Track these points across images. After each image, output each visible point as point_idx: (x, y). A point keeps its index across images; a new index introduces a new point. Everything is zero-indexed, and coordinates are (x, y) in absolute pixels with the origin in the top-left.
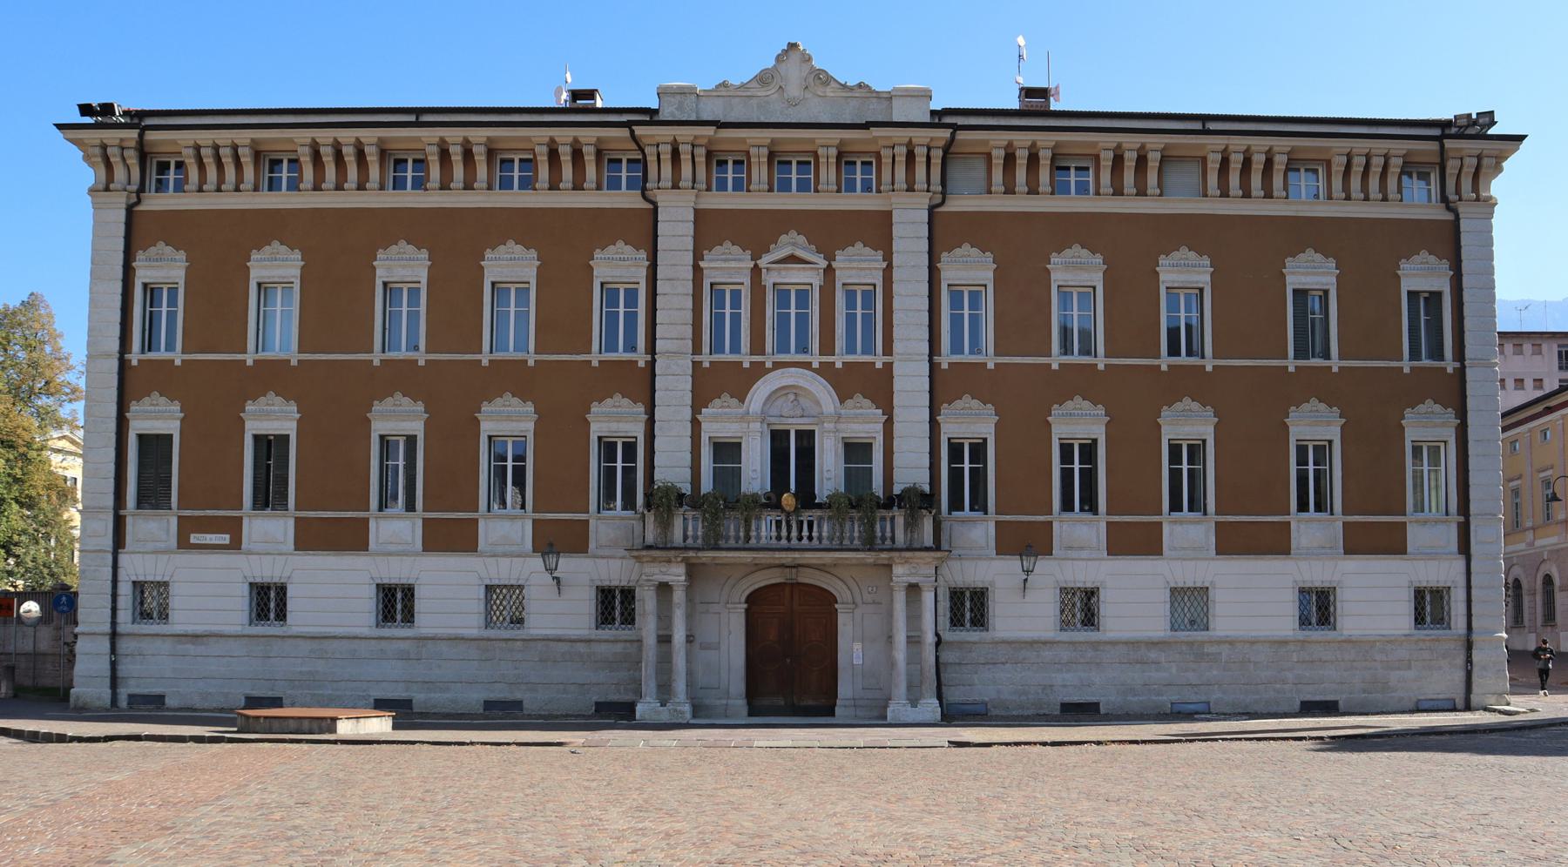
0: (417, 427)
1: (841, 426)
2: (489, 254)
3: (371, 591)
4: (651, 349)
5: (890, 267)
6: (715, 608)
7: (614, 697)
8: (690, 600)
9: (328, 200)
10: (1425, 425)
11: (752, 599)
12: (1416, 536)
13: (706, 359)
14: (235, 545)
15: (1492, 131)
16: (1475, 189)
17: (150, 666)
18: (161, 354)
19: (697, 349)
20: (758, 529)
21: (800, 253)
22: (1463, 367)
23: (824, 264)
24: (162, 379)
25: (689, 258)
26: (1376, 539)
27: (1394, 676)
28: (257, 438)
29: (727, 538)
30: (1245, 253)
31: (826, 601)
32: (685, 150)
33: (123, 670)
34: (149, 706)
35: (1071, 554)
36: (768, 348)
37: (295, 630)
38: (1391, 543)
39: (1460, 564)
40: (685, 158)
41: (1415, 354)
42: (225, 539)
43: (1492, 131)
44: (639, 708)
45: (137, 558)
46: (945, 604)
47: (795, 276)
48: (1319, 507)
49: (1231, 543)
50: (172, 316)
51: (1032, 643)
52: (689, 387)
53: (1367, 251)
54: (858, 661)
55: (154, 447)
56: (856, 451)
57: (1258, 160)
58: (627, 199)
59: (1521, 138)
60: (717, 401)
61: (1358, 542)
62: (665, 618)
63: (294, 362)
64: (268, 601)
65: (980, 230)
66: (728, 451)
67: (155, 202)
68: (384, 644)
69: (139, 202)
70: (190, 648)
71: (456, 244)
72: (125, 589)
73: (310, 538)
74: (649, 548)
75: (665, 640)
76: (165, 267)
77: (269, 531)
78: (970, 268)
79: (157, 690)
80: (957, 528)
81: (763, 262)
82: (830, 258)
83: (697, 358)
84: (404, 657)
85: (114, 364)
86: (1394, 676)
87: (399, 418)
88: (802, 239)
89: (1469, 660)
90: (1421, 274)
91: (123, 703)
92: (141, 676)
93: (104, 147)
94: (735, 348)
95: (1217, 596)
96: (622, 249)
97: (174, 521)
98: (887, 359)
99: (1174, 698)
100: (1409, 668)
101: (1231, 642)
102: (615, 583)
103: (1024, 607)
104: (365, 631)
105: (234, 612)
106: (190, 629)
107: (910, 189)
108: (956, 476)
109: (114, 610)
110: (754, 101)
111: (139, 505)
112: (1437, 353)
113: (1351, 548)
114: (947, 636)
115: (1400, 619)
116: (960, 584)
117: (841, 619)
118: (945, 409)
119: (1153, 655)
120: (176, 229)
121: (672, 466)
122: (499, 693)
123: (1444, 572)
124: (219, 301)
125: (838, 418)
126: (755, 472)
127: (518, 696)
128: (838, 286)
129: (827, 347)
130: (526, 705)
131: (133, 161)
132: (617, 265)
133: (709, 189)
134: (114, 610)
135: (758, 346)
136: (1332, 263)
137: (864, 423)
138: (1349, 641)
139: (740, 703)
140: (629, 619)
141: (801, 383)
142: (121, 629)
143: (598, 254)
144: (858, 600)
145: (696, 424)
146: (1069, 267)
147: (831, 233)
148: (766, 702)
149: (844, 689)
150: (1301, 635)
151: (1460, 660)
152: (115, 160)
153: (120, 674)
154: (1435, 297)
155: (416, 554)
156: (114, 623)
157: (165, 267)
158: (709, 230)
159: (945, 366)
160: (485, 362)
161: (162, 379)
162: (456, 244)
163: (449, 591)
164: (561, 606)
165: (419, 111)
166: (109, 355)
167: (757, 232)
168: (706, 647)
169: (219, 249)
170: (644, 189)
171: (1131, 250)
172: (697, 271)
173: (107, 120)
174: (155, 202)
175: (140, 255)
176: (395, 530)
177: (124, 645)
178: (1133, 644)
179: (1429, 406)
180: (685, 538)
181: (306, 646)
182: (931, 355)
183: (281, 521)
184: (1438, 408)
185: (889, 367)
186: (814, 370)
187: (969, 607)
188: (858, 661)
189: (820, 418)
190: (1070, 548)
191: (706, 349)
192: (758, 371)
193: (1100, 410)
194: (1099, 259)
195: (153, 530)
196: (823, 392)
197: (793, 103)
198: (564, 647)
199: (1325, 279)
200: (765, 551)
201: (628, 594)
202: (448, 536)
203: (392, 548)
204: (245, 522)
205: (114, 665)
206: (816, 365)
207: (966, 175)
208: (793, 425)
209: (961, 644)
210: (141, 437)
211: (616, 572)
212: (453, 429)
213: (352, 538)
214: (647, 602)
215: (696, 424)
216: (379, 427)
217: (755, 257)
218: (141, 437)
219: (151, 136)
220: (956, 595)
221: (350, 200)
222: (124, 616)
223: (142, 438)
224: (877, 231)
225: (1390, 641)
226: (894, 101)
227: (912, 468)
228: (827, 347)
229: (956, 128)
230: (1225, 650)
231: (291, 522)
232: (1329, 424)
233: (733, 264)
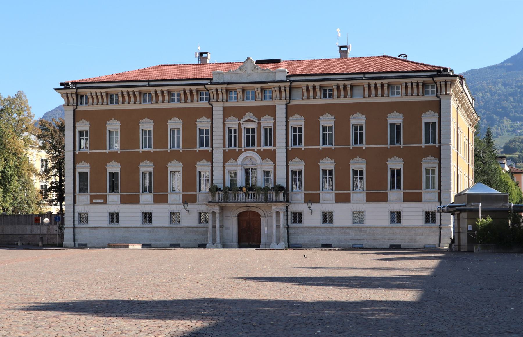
0: (152, 170)
1: (262, 167)
2: (169, 121)
3: (140, 215)
4: (212, 147)
5: (275, 122)
6: (229, 218)
7: (203, 243)
9: (126, 107)
11: (240, 216)
13: (227, 149)
14: (105, 202)
16: (446, 91)
17: (83, 236)
19: (224, 147)
20: (238, 197)
21: (251, 119)
22: (441, 146)
23: (257, 122)
25: (222, 121)
26: (413, 197)
27: (418, 238)
28: (110, 173)
29: (230, 199)
30: (376, 113)
31: (258, 215)
32: (219, 91)
33: (76, 237)
34: (84, 246)
35: (325, 202)
36: (243, 146)
37: (121, 225)
38: (418, 198)
40: (220, 93)
41: (427, 141)
42: (102, 201)
44: (207, 245)
45: (79, 206)
47: (250, 125)
51: (314, 227)
52: (222, 157)
53: (412, 111)
54: (266, 232)
55: (83, 176)
56: (267, 173)
57: (379, 86)
58: (204, 104)
61: (408, 198)
63: (119, 152)
64: (114, 218)
65: (300, 110)
67: (82, 108)
68: (144, 229)
69: (76, 108)
70: (94, 231)
72: (77, 215)
73: (125, 200)
75: (214, 227)
76: (84, 126)
77: (114, 198)
79: (85, 242)
80: (294, 195)
81: (241, 122)
82: (259, 120)
83: (224, 149)
84: (149, 232)
86: (418, 238)
87: (147, 167)
88: (252, 114)
89: (441, 234)
90: (429, 117)
91: (77, 246)
93: (67, 94)
94: (235, 145)
95: (366, 214)
96: (204, 119)
97: (89, 196)
98: (275, 148)
99: (353, 243)
100: (423, 235)
101: (370, 227)
103: (312, 218)
104: (139, 225)
105: (105, 221)
106: (94, 226)
107: (280, 99)
109: (74, 221)
110: (238, 75)
111: (79, 193)
112: (434, 142)
113: (405, 200)
114: (290, 225)
115: (420, 220)
117: (262, 220)
118: (290, 162)
119: (348, 231)
120: (87, 115)
122: (174, 242)
125: (261, 165)
126: (240, 181)
127: (179, 242)
128: (262, 127)
130: (181, 245)
131: (74, 97)
132: (203, 123)
133: (227, 101)
134: (74, 221)
135: (240, 146)
136: (401, 115)
137: (269, 166)
138: (404, 227)
139: (236, 244)
141: (251, 155)
142: (76, 226)
143: (198, 120)
144: (266, 215)
145: (224, 167)
146: (324, 120)
147: (259, 112)
148: (243, 244)
149: (263, 240)
150: (390, 225)
151: (438, 233)
152: (70, 97)
153: (76, 238)
154: (434, 124)
155: (152, 204)
156: (74, 224)
158: (227, 112)
159: (290, 149)
160: (169, 151)
162: (160, 117)
163: (161, 214)
164: (189, 218)
165: (149, 81)
166: (71, 151)
167: (239, 112)
168: (227, 229)
169: (98, 120)
170: (209, 102)
171: (342, 113)
172: (224, 125)
173: (68, 86)
174: (82, 108)
175: (77, 123)
176: (147, 198)
177: (77, 230)
178: (342, 228)
179: (430, 157)
180: (219, 199)
181: (124, 230)
183: (117, 196)
184: (432, 158)
185: (275, 150)
186: (256, 152)
187: (298, 217)
188: (266, 232)
189: (256, 164)
190: (325, 200)
191: (227, 146)
192: (241, 152)
193: (333, 161)
194: (333, 117)
195: (83, 198)
196: (257, 158)
197: (249, 75)
198: (191, 229)
199: (399, 120)
200: (241, 203)
202: (161, 199)
203: (146, 203)
204: (107, 196)
205: (74, 236)
206: (256, 150)
207: (297, 93)
209: (295, 227)
210: (79, 173)
213: (135, 200)
215: (224, 167)
216: (142, 170)
218: (79, 173)
219: (79, 91)
220: (294, 214)
221: (132, 107)
222: (77, 222)
224: (271, 111)
225: (417, 227)
226: (277, 74)
228: (259, 145)
230: (368, 230)
231: (119, 196)
232: (399, 163)
233: (233, 122)
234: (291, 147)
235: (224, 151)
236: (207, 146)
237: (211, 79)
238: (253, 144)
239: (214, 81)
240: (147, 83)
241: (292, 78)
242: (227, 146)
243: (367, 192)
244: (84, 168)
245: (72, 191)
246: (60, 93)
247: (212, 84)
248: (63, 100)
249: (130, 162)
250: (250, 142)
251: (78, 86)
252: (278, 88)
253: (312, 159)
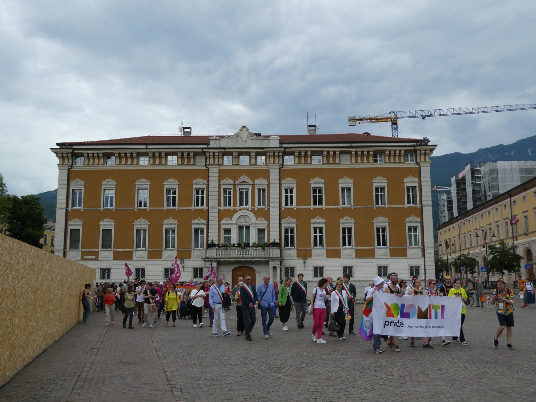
10: (411, 221)
12: (410, 252)
13: (222, 208)
15: (429, 144)
18: (77, 207)
19: (219, 206)
24: (77, 214)
25: (217, 182)
35: (317, 258)
38: (403, 254)
39: (423, 259)
41: (409, 203)
42: (94, 257)
43: (429, 144)
46: (283, 272)
48: (384, 244)
49: (359, 254)
50: (80, 198)
53: (395, 176)
55: (75, 233)
56: (261, 231)
59: (436, 146)
60: (225, 219)
66: (227, 231)
69: (71, 168)
71: (156, 178)
76: (78, 184)
78: (290, 183)
82: (254, 181)
85: (64, 211)
88: (246, 177)
93: (62, 154)
94: (230, 205)
97: (80, 252)
108: (287, 237)
111: (70, 248)
116: (288, 266)
117: (257, 275)
121: (213, 237)
123: (419, 262)
124: (93, 193)
128: (256, 189)
129: (253, 205)
137: (262, 223)
147: (254, 174)
154: (414, 188)
157: (78, 184)
158: (222, 174)
159: (283, 209)
161: (77, 214)
167: (234, 174)
169: (93, 180)
182: (280, 206)
185: (269, 209)
191: (222, 206)
192: (235, 211)
196: (252, 216)
201: (201, 270)
206: (250, 209)
211: (199, 264)
212: (155, 227)
217: (234, 182)
219: (75, 151)
220: (287, 269)
223: (71, 230)
224: (265, 174)
227: (275, 236)
228: (253, 205)
229: (286, 148)
231: (112, 252)
234: (284, 207)
235: (219, 210)
236: (202, 204)
238: (247, 204)
241: (284, 146)
242: (222, 206)
243: (357, 248)
244: (76, 224)
245: (62, 247)
246: (56, 153)
248: (58, 160)
249: (125, 220)
250: (243, 200)
251: (74, 147)
252: (272, 154)
253: (304, 217)
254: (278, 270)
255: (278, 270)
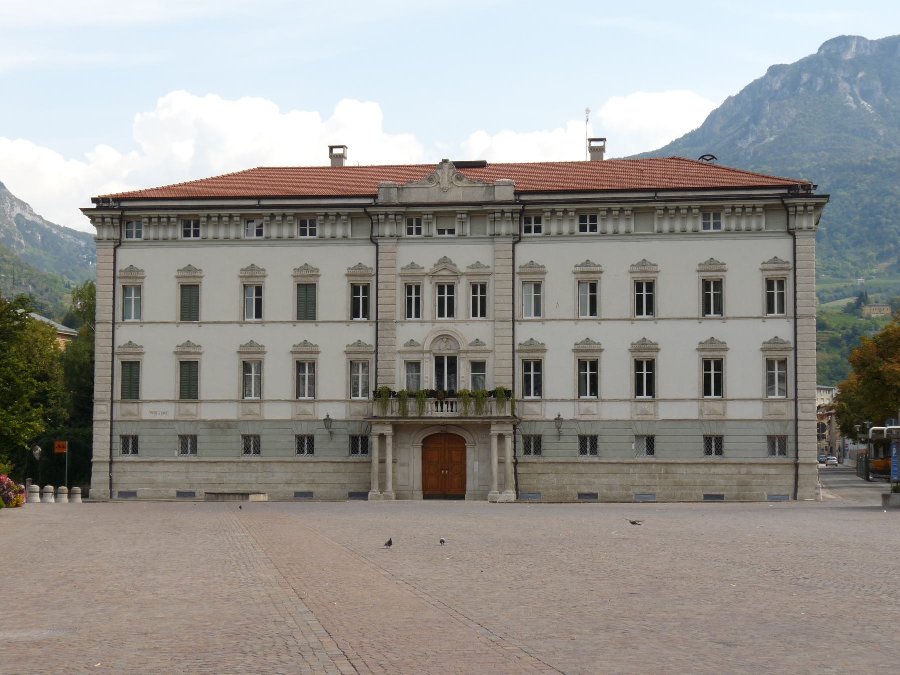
8: (394, 441)
11: (425, 441)
44: (370, 494)
54: (476, 470)
62: (383, 450)
74: (376, 417)
75: (383, 462)
92: (125, 482)
102: (358, 434)
114: (522, 458)
122: (303, 489)
139: (420, 494)
140: (366, 450)
165: (260, 198)
188: (476, 470)
197: (444, 191)
208: (446, 353)
214: (375, 442)
219: (127, 213)
220: (527, 439)
226: (496, 189)
229: (525, 203)
237: (375, 197)
239: (381, 199)
240: (254, 203)
241: (524, 198)
246: (90, 216)
247: (377, 206)
251: (124, 204)
254: (509, 442)
255: (509, 442)
